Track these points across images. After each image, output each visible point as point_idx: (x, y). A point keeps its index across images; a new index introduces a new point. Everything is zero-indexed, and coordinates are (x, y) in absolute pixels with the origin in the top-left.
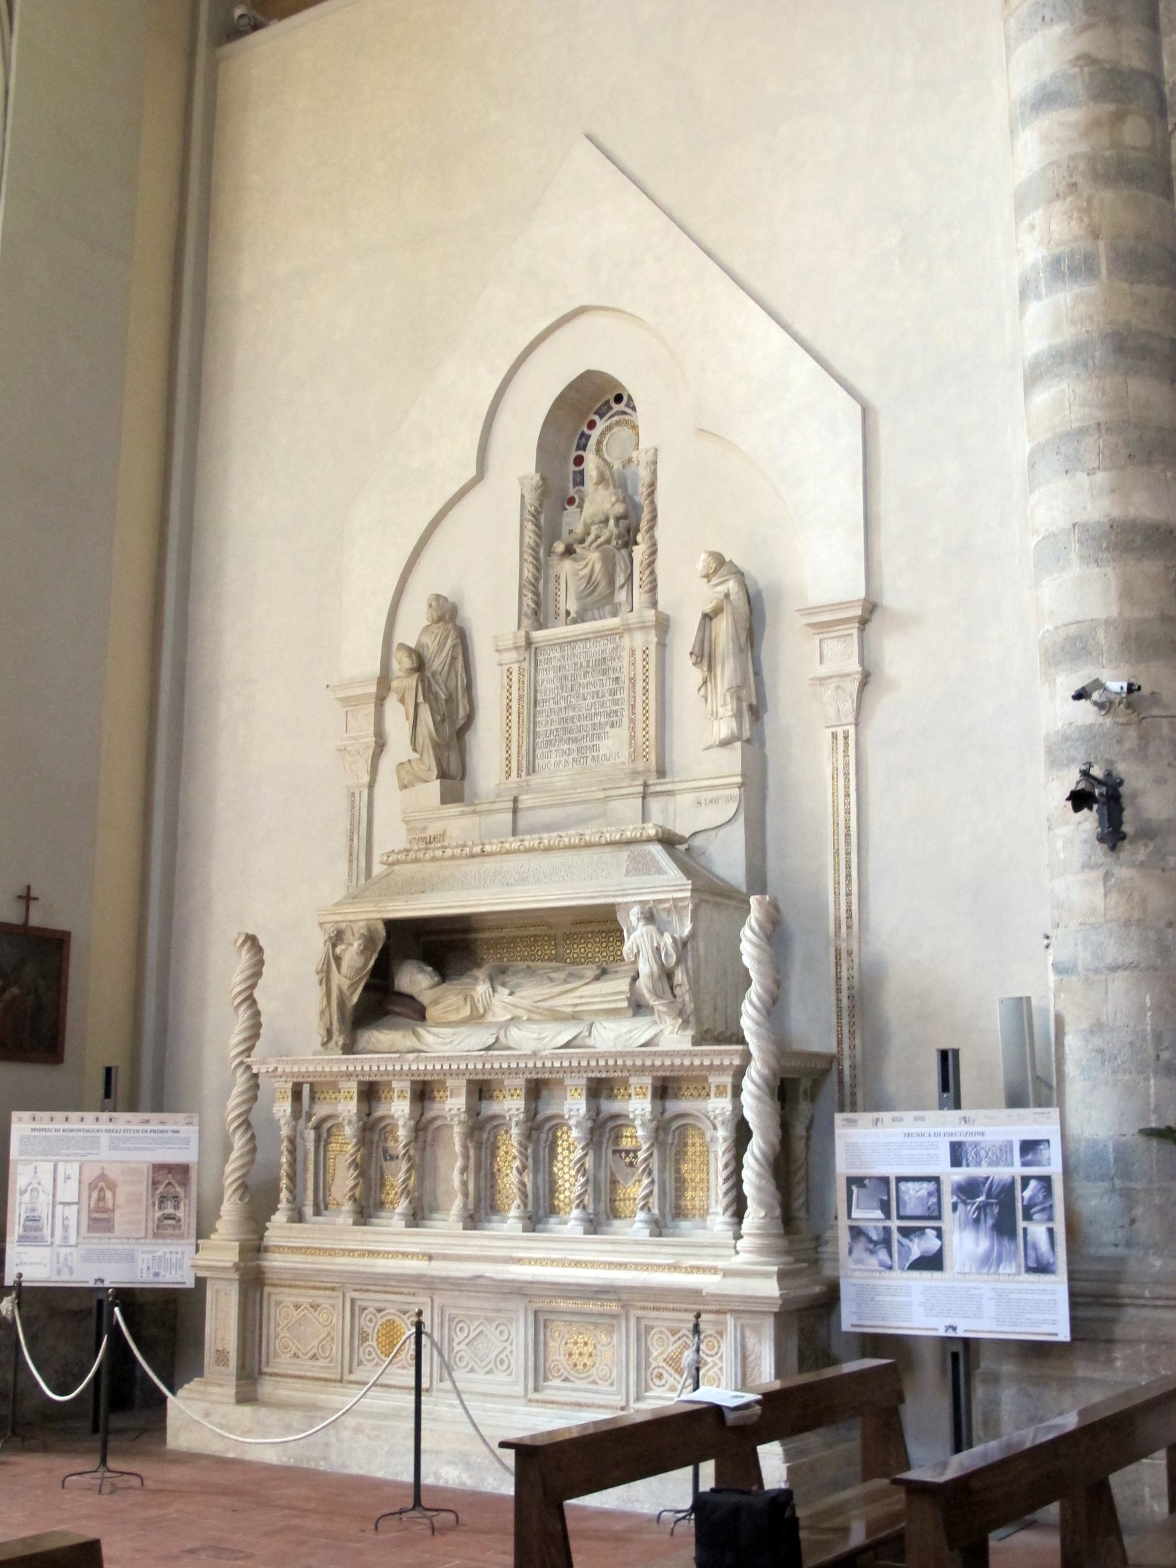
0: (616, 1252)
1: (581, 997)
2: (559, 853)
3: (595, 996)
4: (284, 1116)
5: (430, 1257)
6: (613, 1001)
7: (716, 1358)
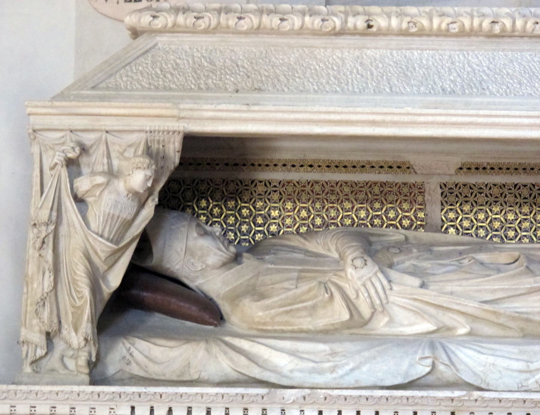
2: (525, 44)
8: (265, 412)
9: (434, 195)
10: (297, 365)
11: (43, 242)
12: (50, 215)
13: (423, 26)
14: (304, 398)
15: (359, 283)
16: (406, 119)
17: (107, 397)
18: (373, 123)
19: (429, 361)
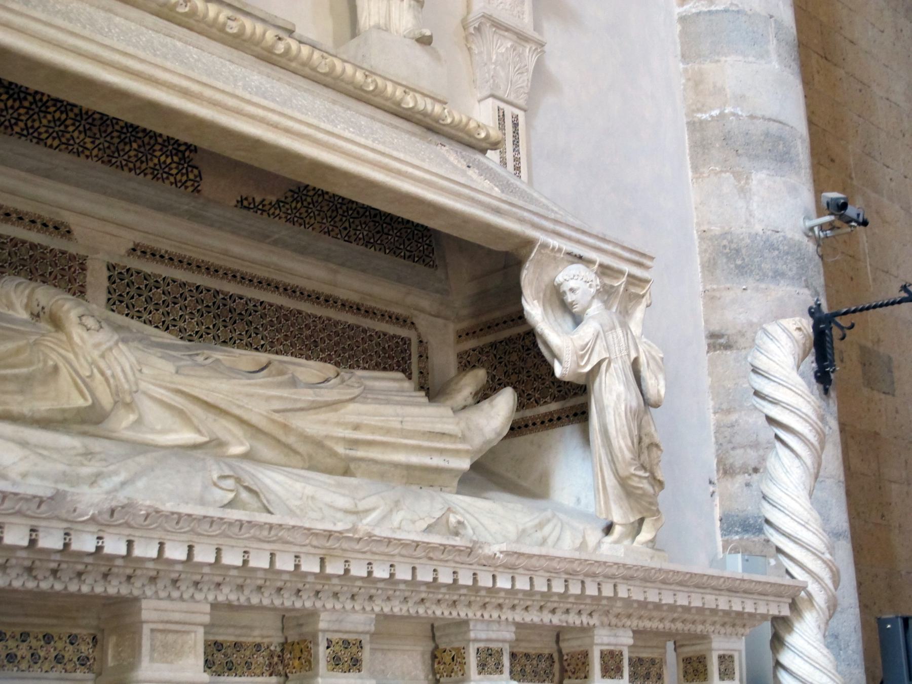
1: (357, 427)
6: (441, 451)
8: (34, 534)
9: (97, 279)
10: (36, 465)
13: (197, 7)
14: (112, 512)
15: (96, 354)
16: (231, 102)
18: (185, 93)
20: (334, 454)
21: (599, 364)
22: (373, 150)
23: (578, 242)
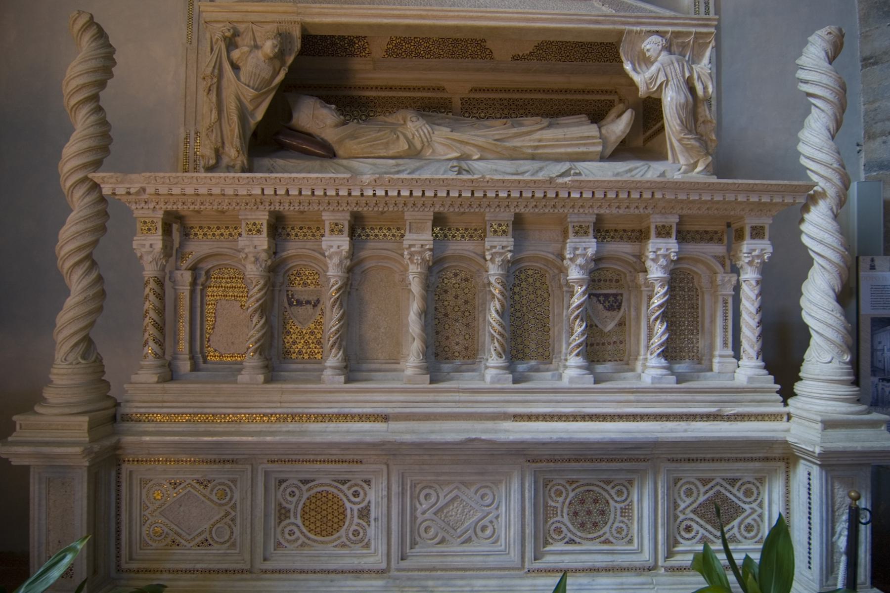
0: (638, 401)
1: (540, 141)
3: (558, 140)
4: (149, 253)
5: (385, 418)
6: (585, 145)
7: (754, 505)
11: (210, 90)
12: (213, 71)
17: (246, 181)
19: (456, 169)
20: (524, 153)
21: (661, 84)
22: (517, 13)
23: (656, 24)
